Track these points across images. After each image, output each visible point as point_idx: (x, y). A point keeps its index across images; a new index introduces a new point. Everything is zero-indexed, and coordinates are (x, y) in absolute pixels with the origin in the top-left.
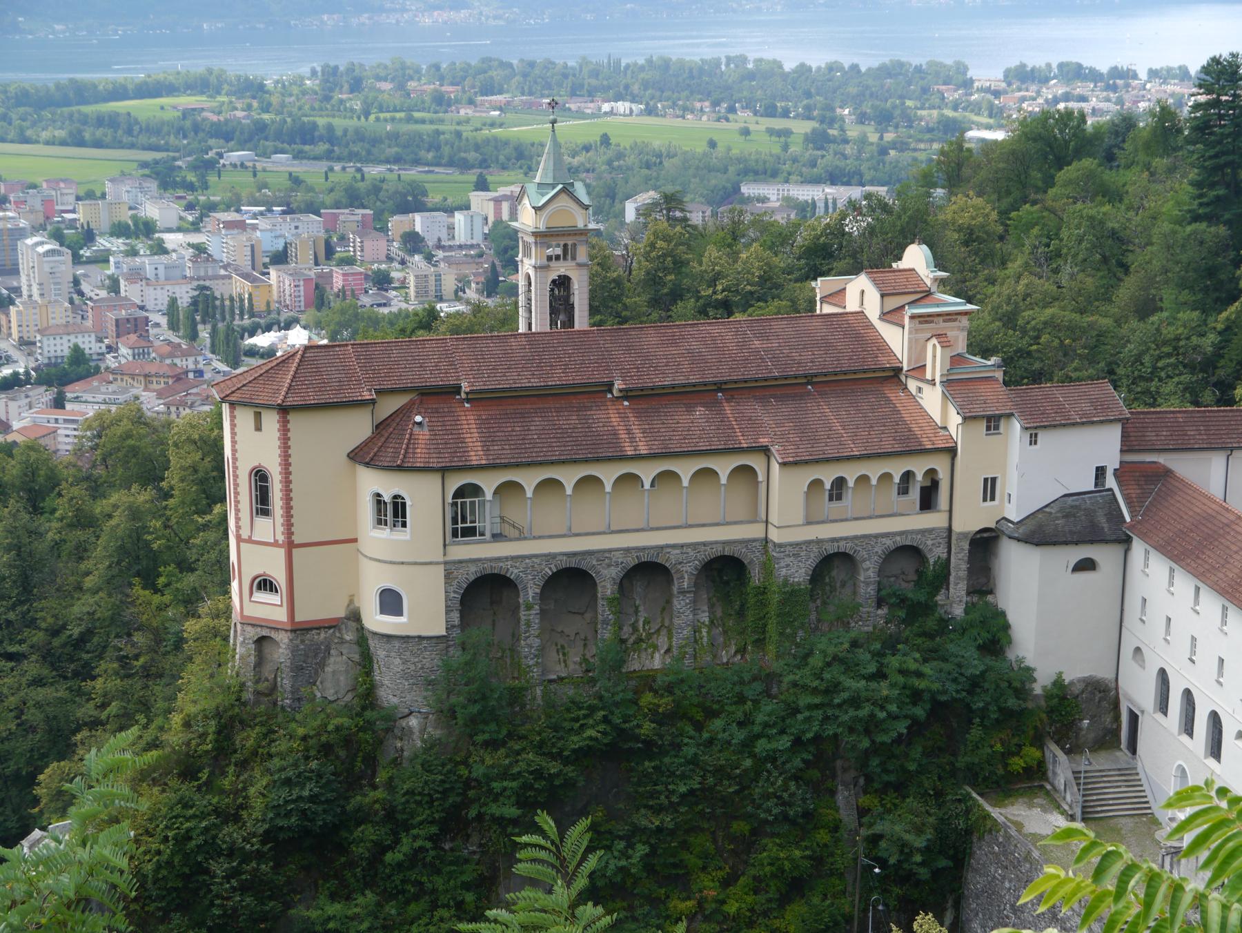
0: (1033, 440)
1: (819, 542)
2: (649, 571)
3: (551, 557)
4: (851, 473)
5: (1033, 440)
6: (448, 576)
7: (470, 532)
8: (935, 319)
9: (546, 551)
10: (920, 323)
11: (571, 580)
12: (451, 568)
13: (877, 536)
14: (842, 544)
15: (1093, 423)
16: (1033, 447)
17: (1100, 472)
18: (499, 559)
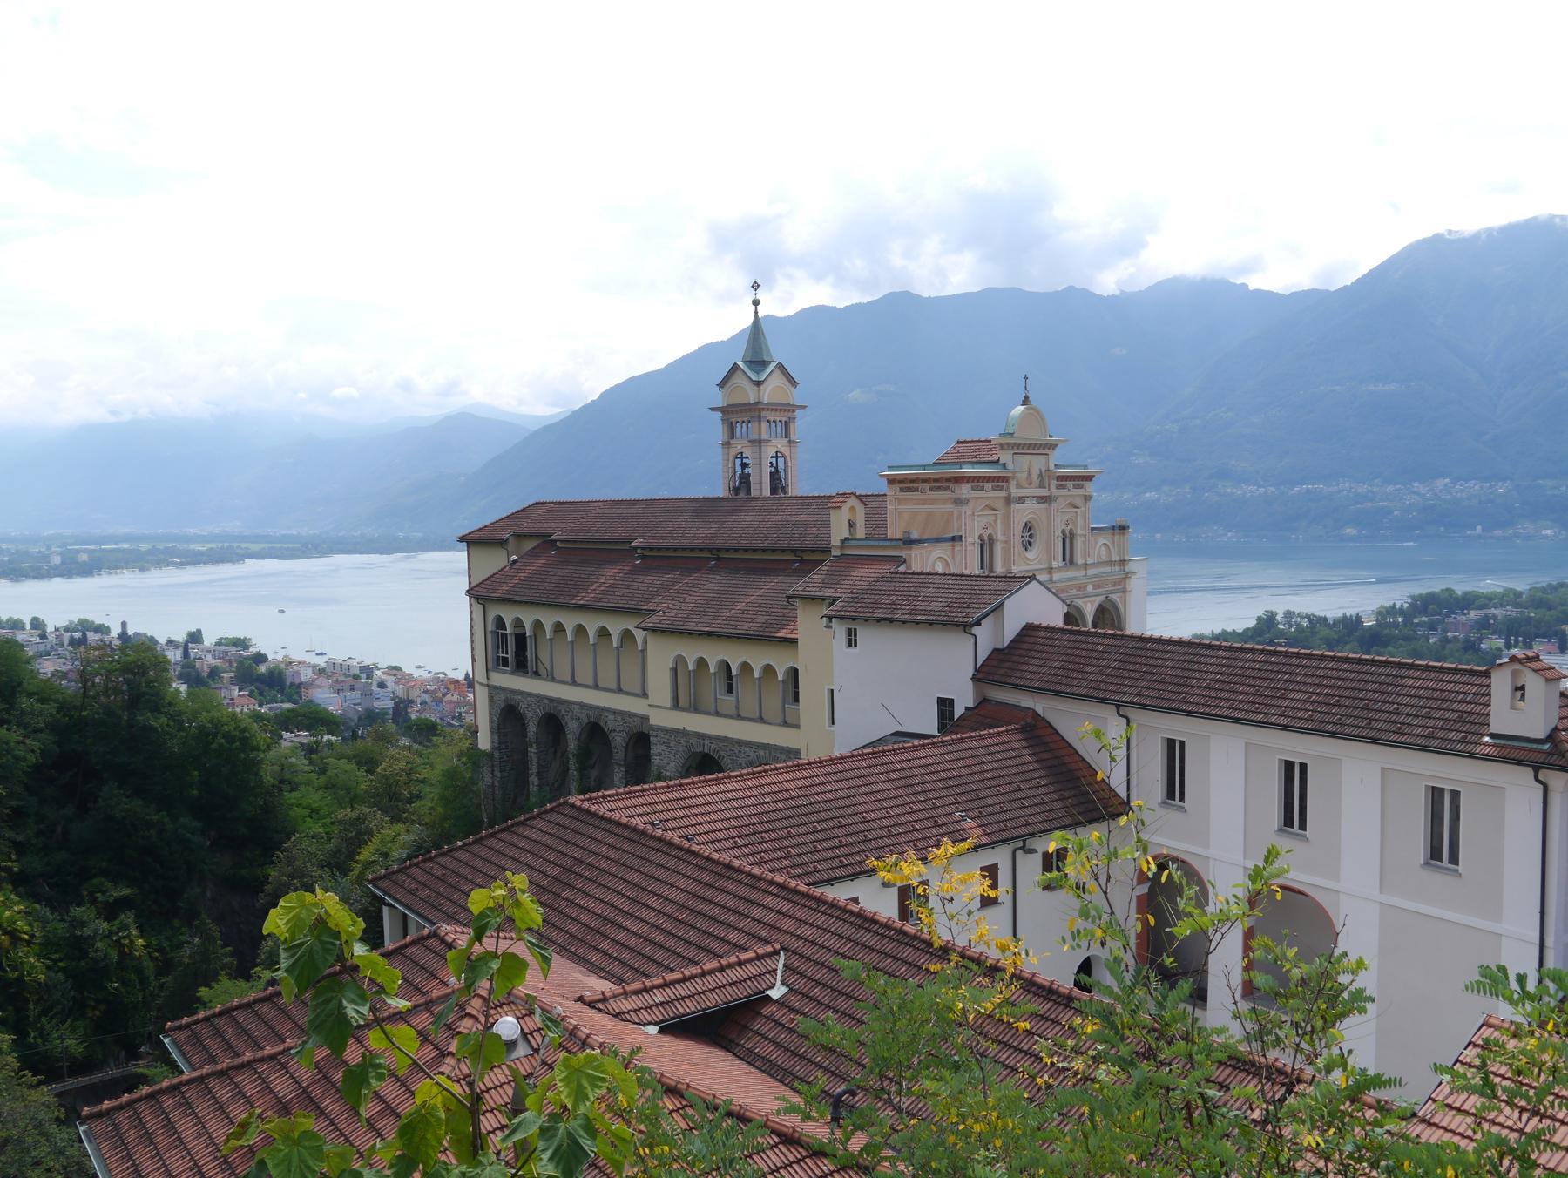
0: (852, 642)
1: (684, 733)
2: (595, 731)
3: (540, 698)
4: (736, 656)
5: (852, 642)
6: (491, 699)
7: (505, 662)
8: (921, 486)
9: (535, 691)
10: (902, 490)
11: (553, 722)
12: (493, 691)
13: (741, 743)
14: (707, 742)
15: (918, 623)
16: (852, 650)
17: (945, 705)
18: (513, 691)
